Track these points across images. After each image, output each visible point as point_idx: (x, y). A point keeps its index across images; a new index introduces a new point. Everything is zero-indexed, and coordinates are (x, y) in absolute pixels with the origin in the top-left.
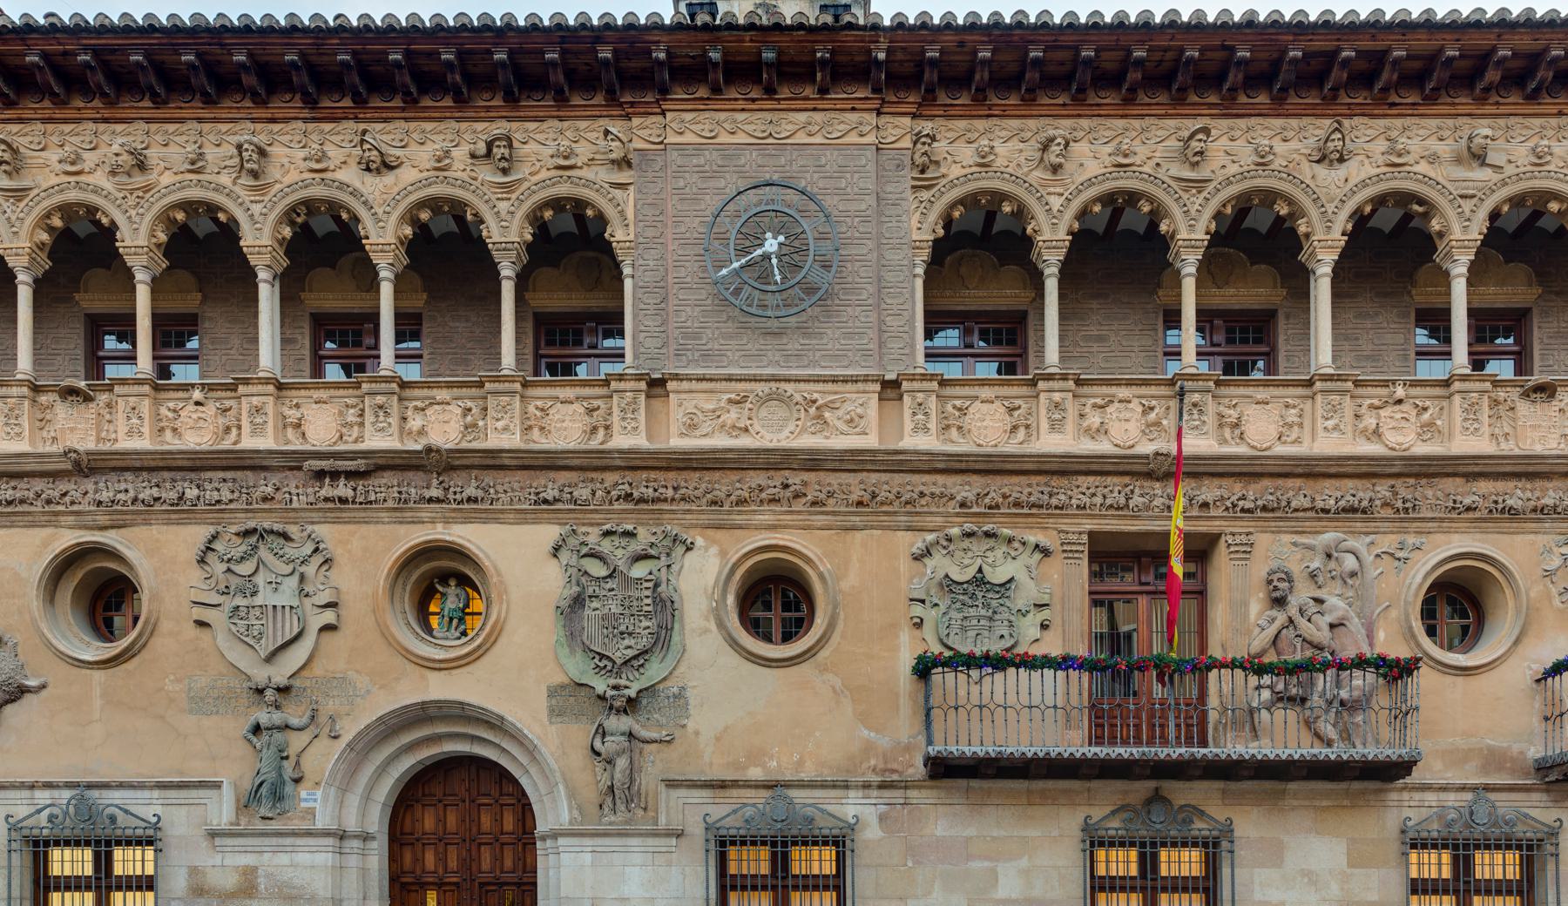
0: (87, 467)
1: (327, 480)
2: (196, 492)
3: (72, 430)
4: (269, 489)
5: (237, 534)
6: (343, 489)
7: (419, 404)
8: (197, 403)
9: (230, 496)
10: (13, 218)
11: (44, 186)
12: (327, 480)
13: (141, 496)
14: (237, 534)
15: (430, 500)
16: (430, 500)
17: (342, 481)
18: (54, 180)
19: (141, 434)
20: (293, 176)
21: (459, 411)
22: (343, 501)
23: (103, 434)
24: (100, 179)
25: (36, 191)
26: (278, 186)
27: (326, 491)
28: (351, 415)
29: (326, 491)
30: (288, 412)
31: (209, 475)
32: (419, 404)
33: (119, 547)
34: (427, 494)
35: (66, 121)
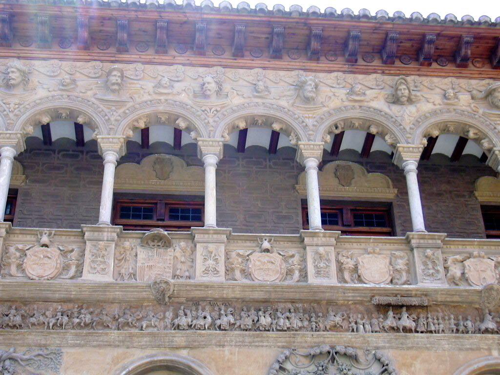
0: (164, 298)
1: (391, 313)
2: (269, 320)
3: (151, 267)
4: (338, 319)
5: (306, 356)
6: (407, 321)
7: (458, 257)
8: (267, 251)
9: (300, 324)
10: (112, 119)
11: (138, 100)
12: (391, 313)
13: (218, 322)
14: (306, 356)
15: (487, 331)
16: (487, 331)
17: (405, 315)
18: (146, 97)
19: (216, 272)
20: (335, 103)
21: (493, 263)
22: (406, 330)
23: (178, 273)
24: (183, 97)
25: (131, 104)
26: (325, 109)
27: (390, 321)
28: (401, 264)
29: (390, 321)
30: (343, 259)
31: (281, 306)
32: (458, 257)
33: (193, 365)
34: (483, 327)
35: (161, 64)
